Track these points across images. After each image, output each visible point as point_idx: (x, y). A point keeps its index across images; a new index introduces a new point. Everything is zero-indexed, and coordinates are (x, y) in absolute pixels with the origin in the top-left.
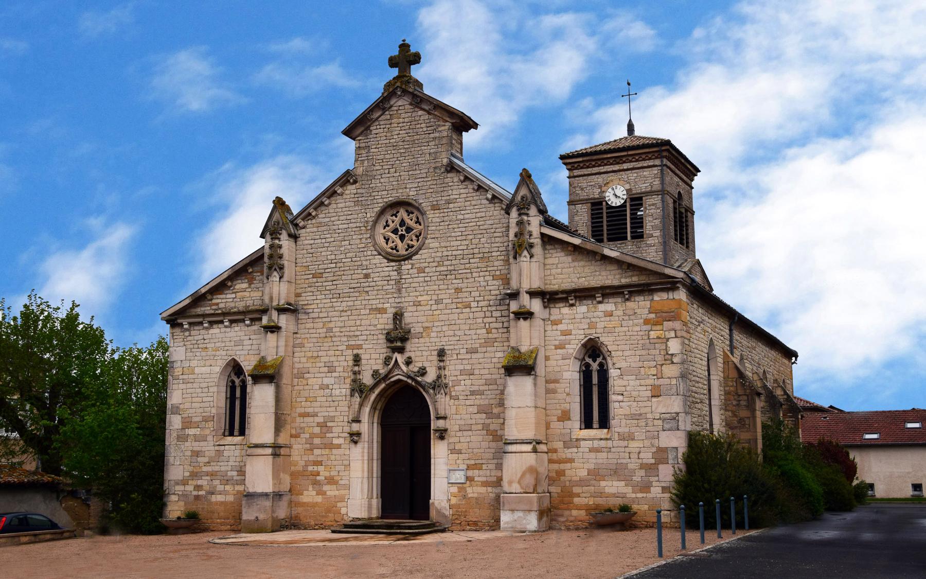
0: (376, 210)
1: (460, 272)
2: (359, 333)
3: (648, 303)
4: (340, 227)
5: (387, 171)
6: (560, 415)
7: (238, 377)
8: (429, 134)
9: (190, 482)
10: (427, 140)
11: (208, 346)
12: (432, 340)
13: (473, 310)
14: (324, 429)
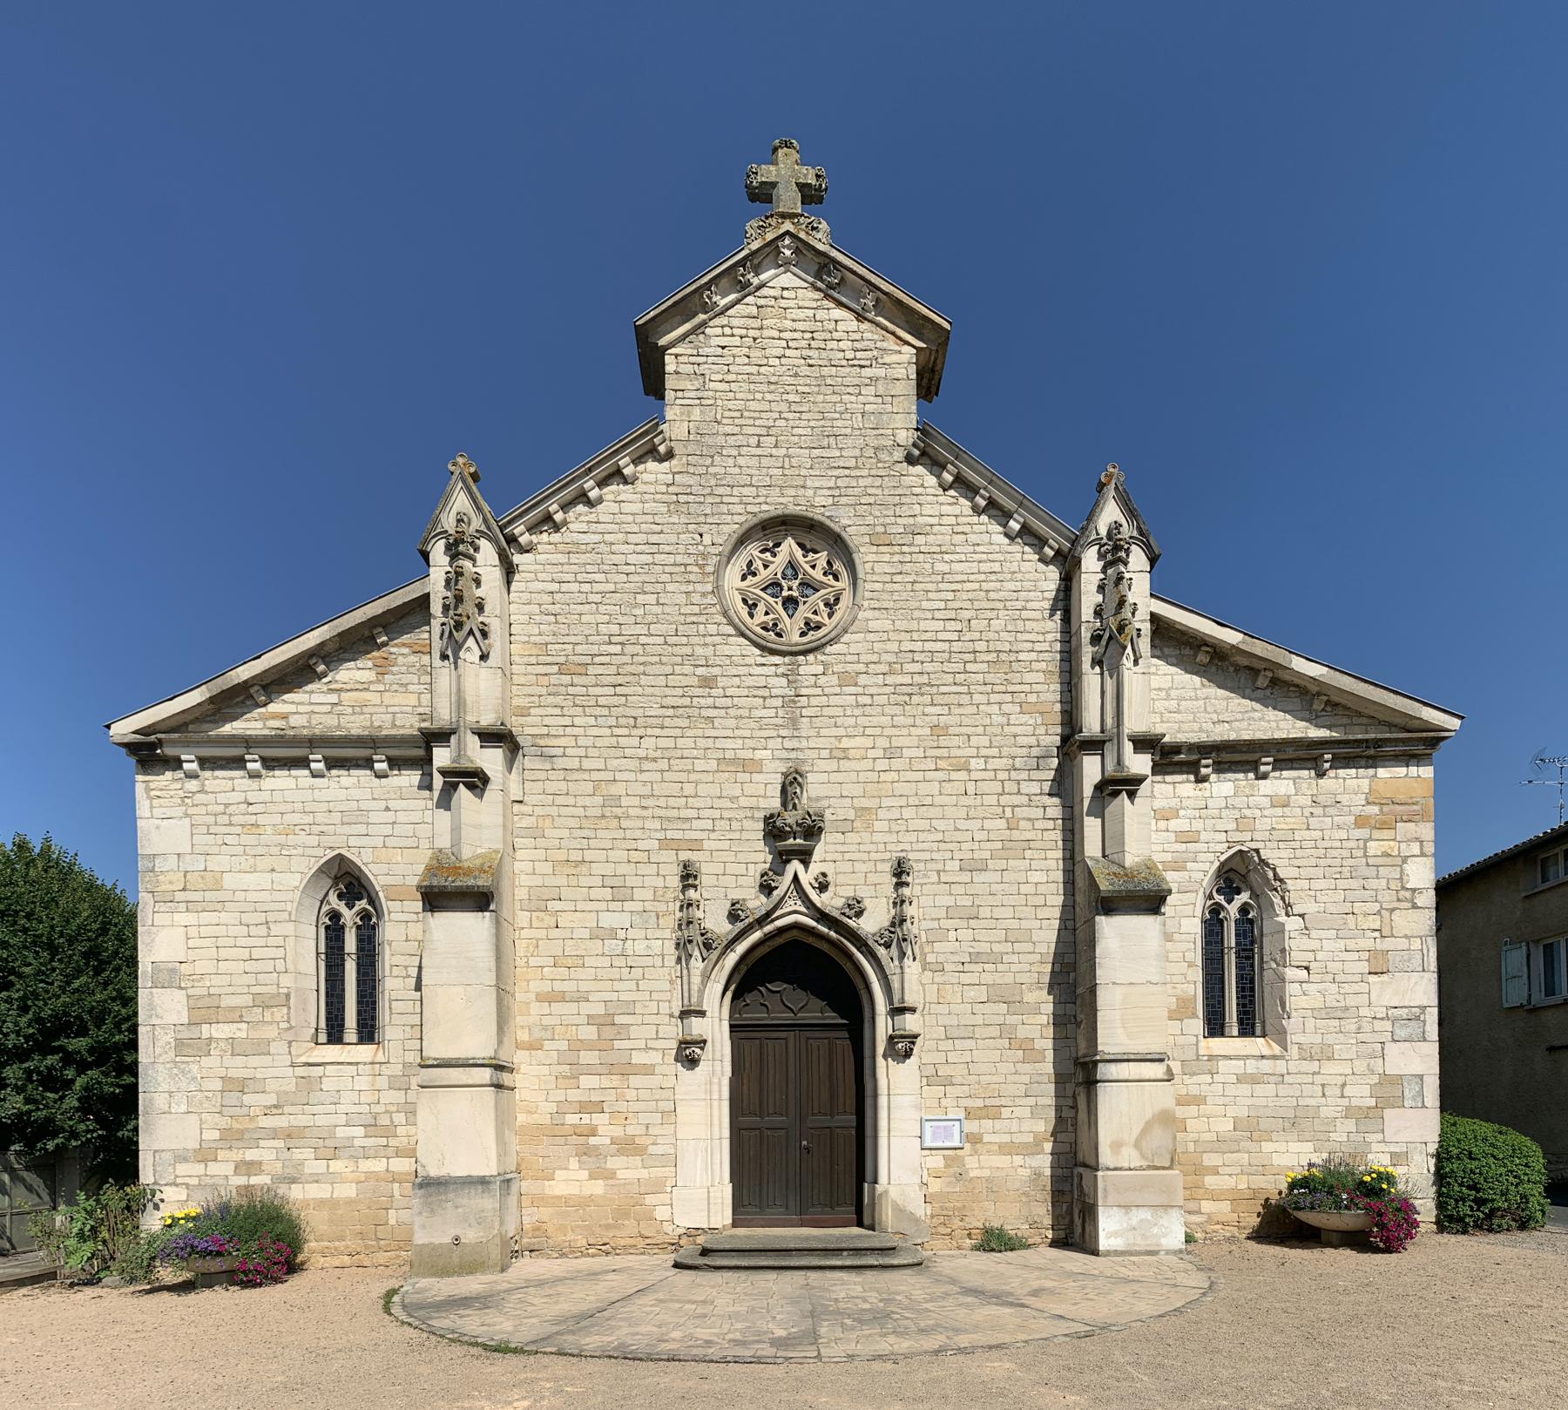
0: (726, 529)
1: (943, 689)
2: (692, 813)
3: (1366, 781)
4: (632, 559)
5: (754, 440)
6: (1174, 1007)
7: (350, 906)
8: (862, 367)
9: (221, 1155)
10: (857, 381)
11: (261, 820)
12: (877, 837)
13: (975, 776)
14: (608, 1032)
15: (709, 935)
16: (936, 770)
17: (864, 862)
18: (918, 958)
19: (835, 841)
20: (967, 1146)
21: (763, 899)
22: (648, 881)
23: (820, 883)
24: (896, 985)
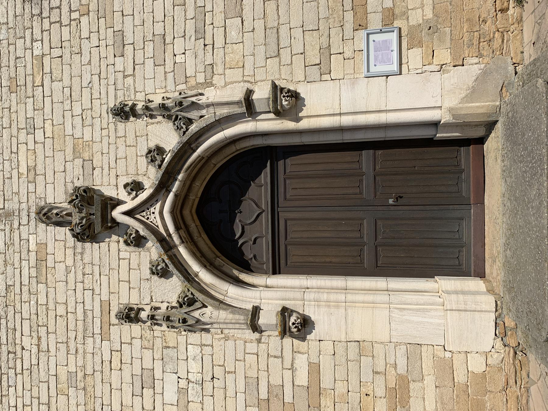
2: (80, 308)
13: (46, 50)
15: (180, 300)
17: (117, 148)
18: (200, 91)
19: (100, 176)
20: (397, 23)
21: (149, 244)
22: (137, 354)
23: (132, 190)
24: (224, 111)
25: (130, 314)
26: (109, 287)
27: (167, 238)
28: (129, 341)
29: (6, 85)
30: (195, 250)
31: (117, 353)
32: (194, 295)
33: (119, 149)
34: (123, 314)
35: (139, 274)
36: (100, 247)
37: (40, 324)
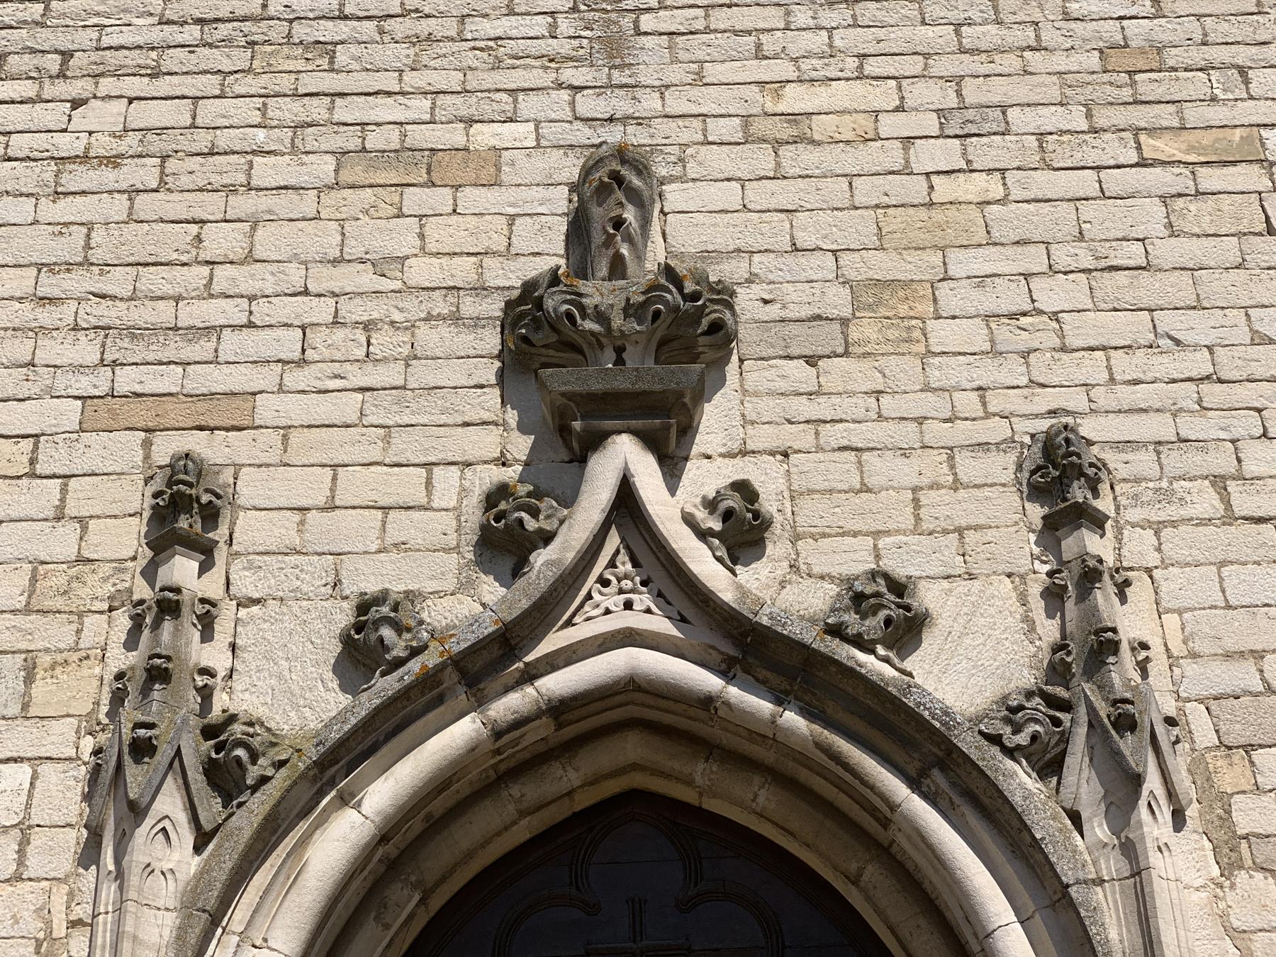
15: (238, 729)
16: (1142, 163)
17: (905, 453)
18: (1192, 812)
19: (782, 385)
21: (491, 589)
23: (728, 515)
25: (189, 511)
26: (309, 426)
27: (520, 665)
28: (71, 510)
29: (1128, 32)
30: (461, 789)
31: (25, 459)
32: (255, 789)
33: (900, 461)
34: (190, 485)
35: (361, 548)
36: (482, 387)
37: (171, 165)
